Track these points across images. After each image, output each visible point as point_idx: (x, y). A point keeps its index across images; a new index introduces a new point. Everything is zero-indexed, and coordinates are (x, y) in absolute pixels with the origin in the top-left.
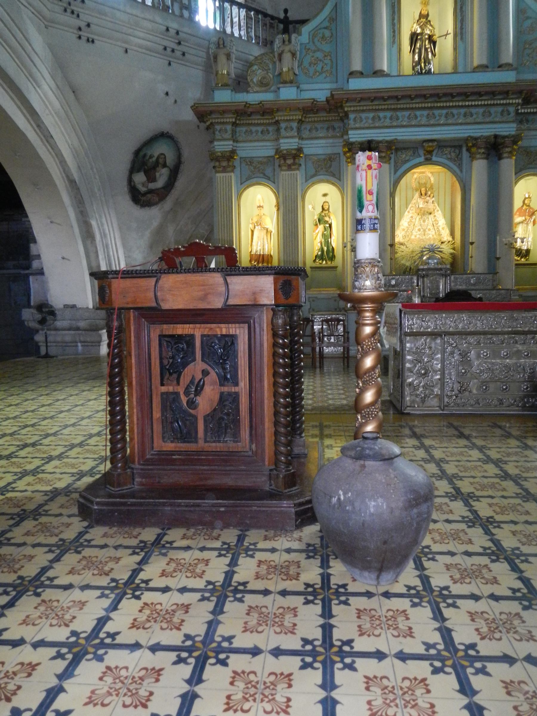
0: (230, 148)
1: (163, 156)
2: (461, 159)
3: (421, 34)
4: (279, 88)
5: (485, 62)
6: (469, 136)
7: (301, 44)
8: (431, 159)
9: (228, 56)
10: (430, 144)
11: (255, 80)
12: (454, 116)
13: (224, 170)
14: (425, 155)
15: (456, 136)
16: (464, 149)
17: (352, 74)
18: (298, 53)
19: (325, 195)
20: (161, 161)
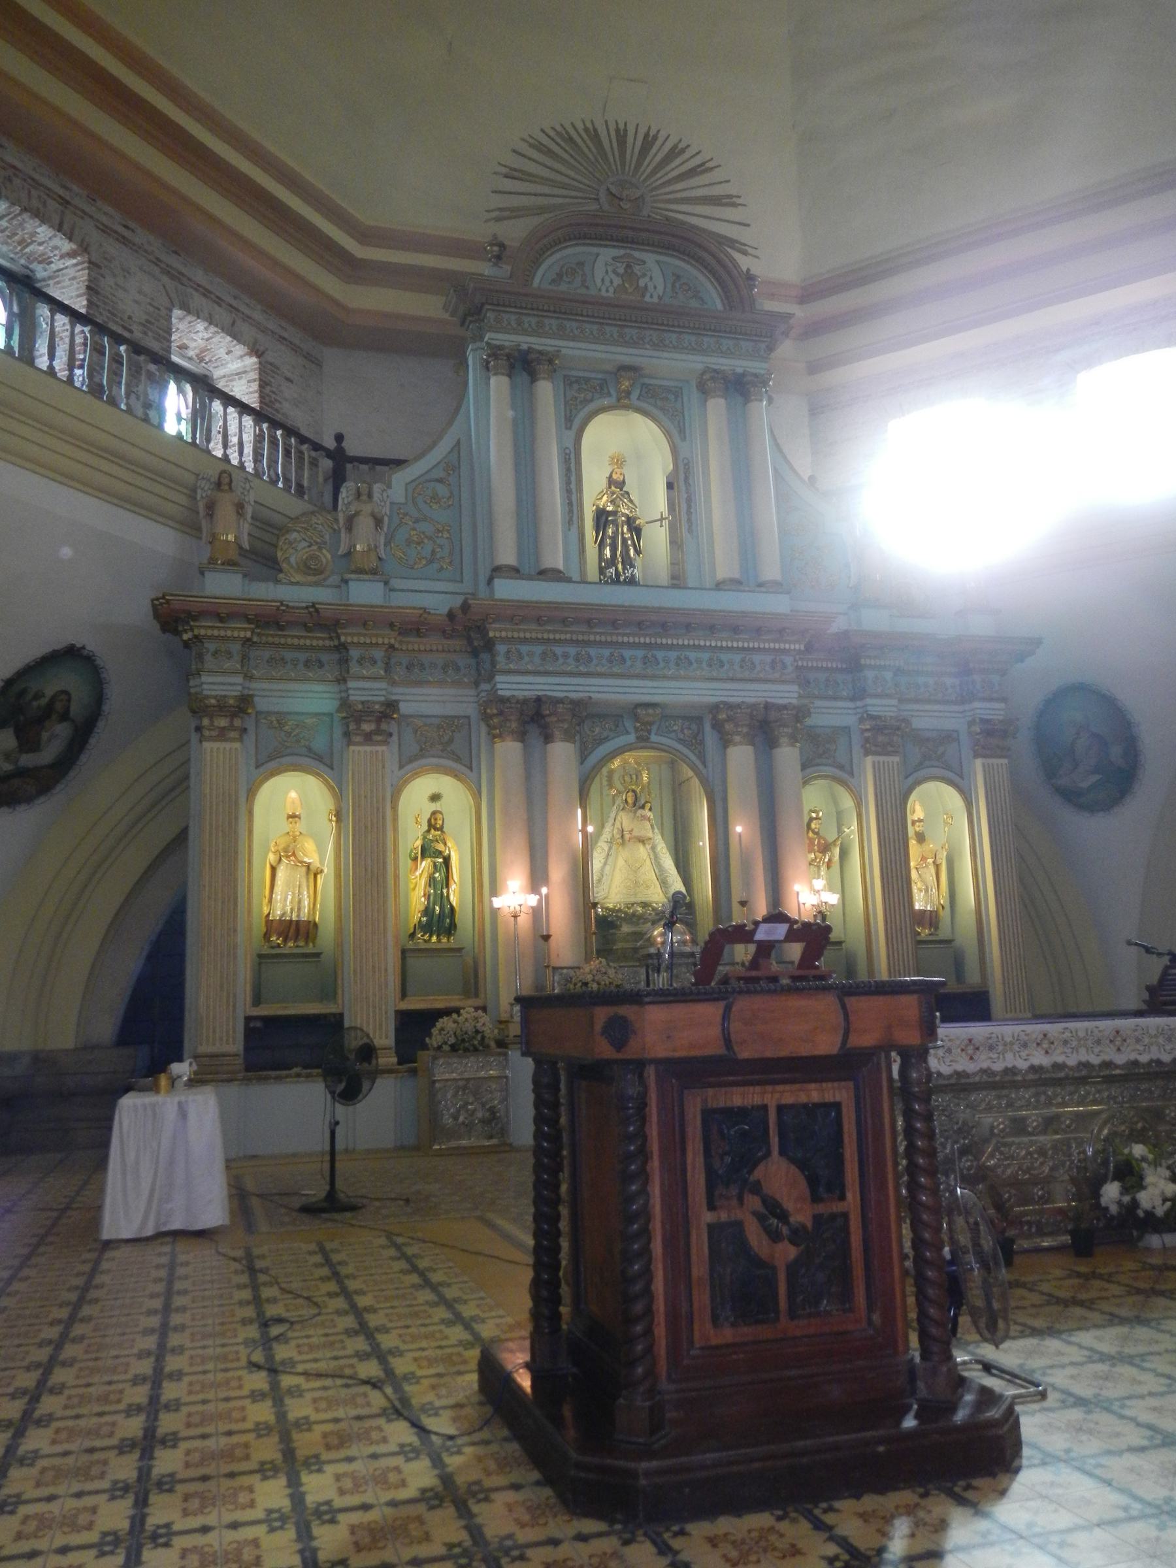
0: (235, 691)
1: (63, 697)
2: (702, 743)
3: (614, 513)
4: (346, 582)
6: (722, 702)
7: (392, 503)
8: (647, 739)
9: (240, 507)
10: (651, 711)
11: (293, 560)
12: (691, 663)
13: (222, 735)
14: (636, 730)
15: (696, 699)
16: (707, 727)
17: (497, 571)
18: (386, 519)
19: (435, 798)
20: (59, 706)
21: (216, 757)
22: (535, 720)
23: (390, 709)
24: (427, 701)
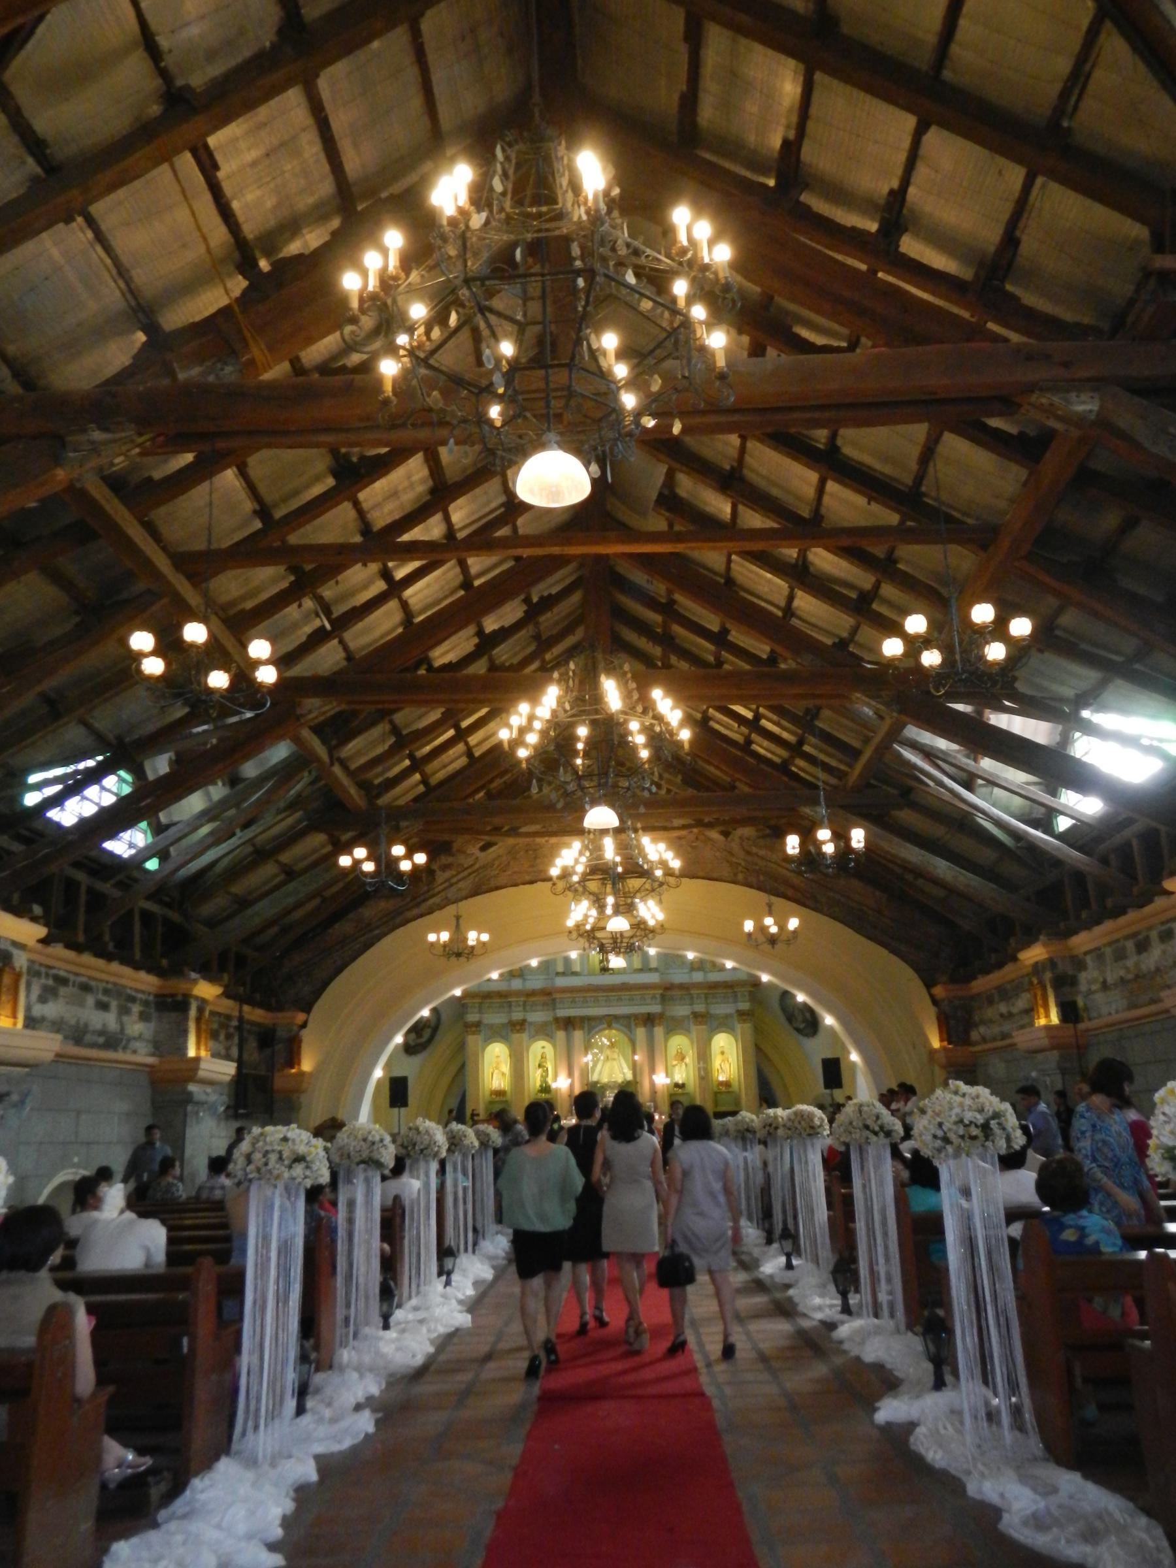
5: (640, 967)
13: (474, 1033)
17: (558, 974)
21: (471, 1039)
22: (568, 1024)
23: (524, 1021)
24: (537, 1016)
